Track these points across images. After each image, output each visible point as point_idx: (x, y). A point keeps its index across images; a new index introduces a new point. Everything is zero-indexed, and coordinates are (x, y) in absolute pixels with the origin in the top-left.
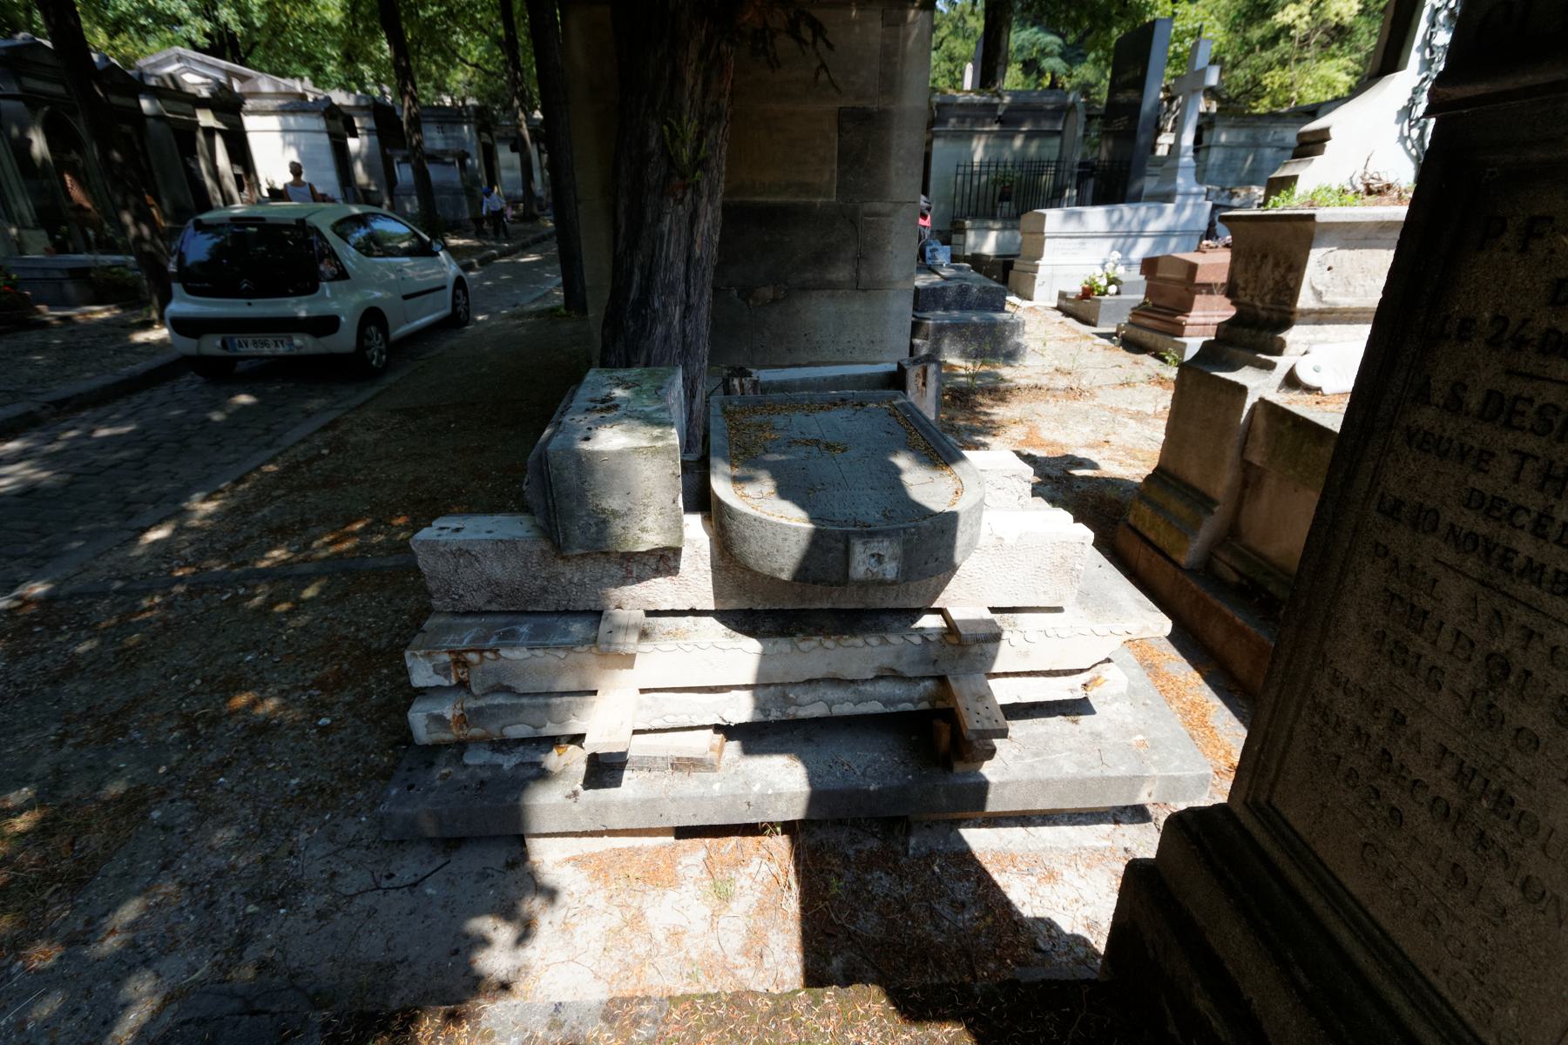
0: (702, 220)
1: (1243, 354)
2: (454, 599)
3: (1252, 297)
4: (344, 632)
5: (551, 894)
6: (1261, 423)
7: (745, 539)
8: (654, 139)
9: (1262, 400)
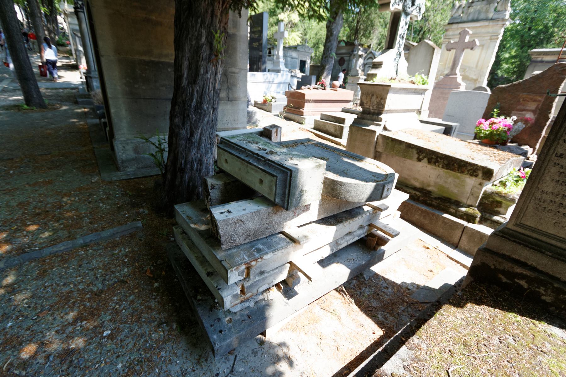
0: (219, 74)
1: (369, 122)
2: (231, 243)
3: (369, 106)
4: (67, 289)
5: (282, 345)
6: (380, 140)
7: (348, 192)
8: (204, 38)
9: (380, 134)
